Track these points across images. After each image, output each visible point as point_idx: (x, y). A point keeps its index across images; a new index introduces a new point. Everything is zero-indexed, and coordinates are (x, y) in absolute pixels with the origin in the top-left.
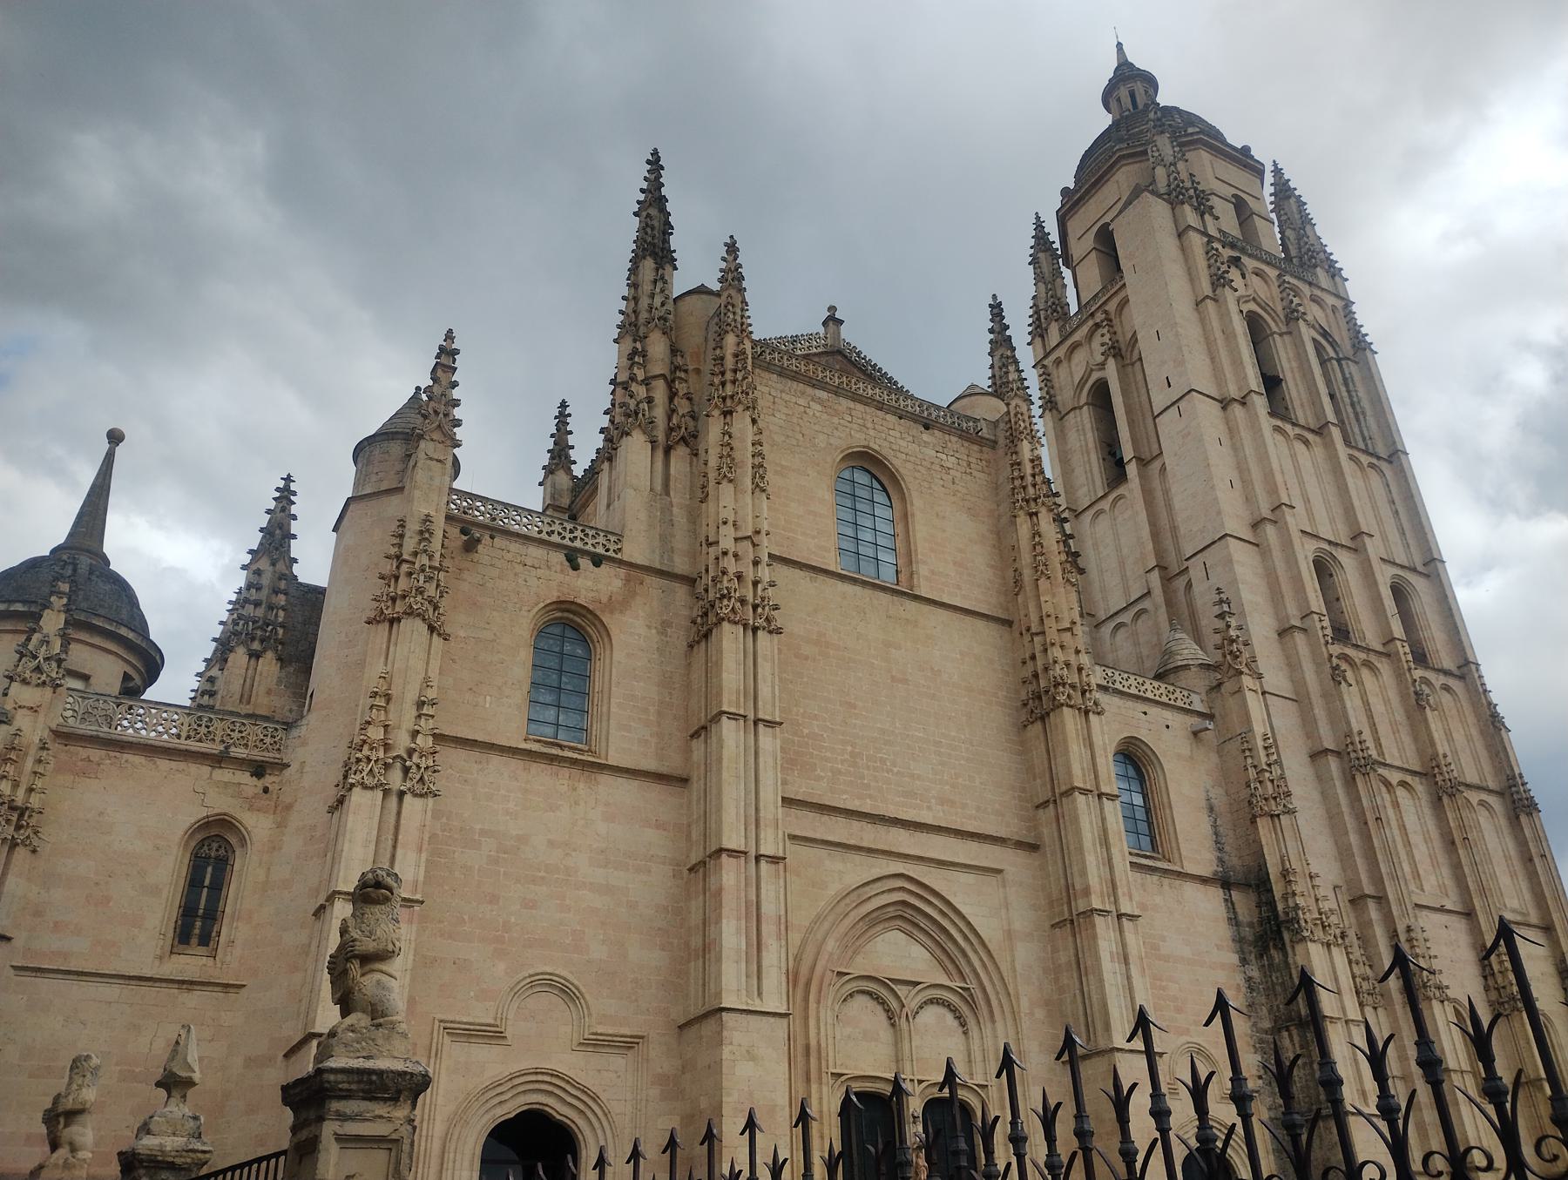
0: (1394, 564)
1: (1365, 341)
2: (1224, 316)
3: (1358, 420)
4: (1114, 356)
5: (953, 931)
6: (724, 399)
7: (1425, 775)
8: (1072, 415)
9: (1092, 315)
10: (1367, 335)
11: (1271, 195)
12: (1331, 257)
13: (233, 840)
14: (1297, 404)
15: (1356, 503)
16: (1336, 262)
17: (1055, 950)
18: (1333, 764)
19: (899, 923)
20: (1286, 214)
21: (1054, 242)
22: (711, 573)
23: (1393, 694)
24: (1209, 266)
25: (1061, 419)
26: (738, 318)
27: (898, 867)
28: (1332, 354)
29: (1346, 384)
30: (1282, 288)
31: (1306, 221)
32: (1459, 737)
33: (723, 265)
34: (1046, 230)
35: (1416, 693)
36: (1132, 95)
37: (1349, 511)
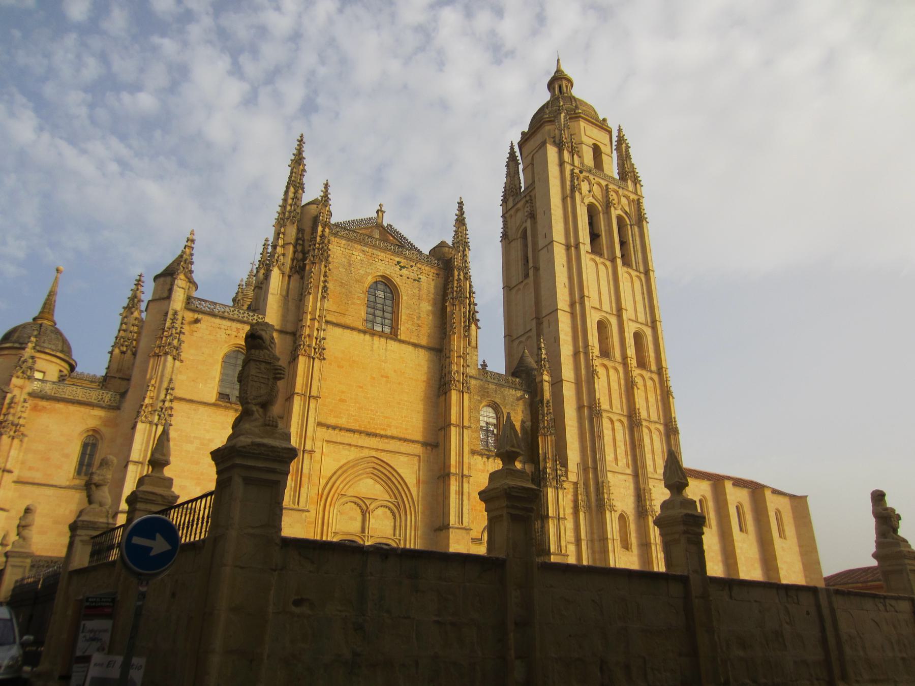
3: (635, 254)
4: (530, 218)
6: (314, 257)
8: (513, 242)
11: (616, 142)
13: (98, 437)
16: (639, 177)
18: (586, 411)
21: (518, 156)
23: (622, 382)
25: (510, 243)
27: (374, 454)
28: (628, 222)
29: (632, 237)
31: (628, 156)
32: (652, 400)
34: (515, 150)
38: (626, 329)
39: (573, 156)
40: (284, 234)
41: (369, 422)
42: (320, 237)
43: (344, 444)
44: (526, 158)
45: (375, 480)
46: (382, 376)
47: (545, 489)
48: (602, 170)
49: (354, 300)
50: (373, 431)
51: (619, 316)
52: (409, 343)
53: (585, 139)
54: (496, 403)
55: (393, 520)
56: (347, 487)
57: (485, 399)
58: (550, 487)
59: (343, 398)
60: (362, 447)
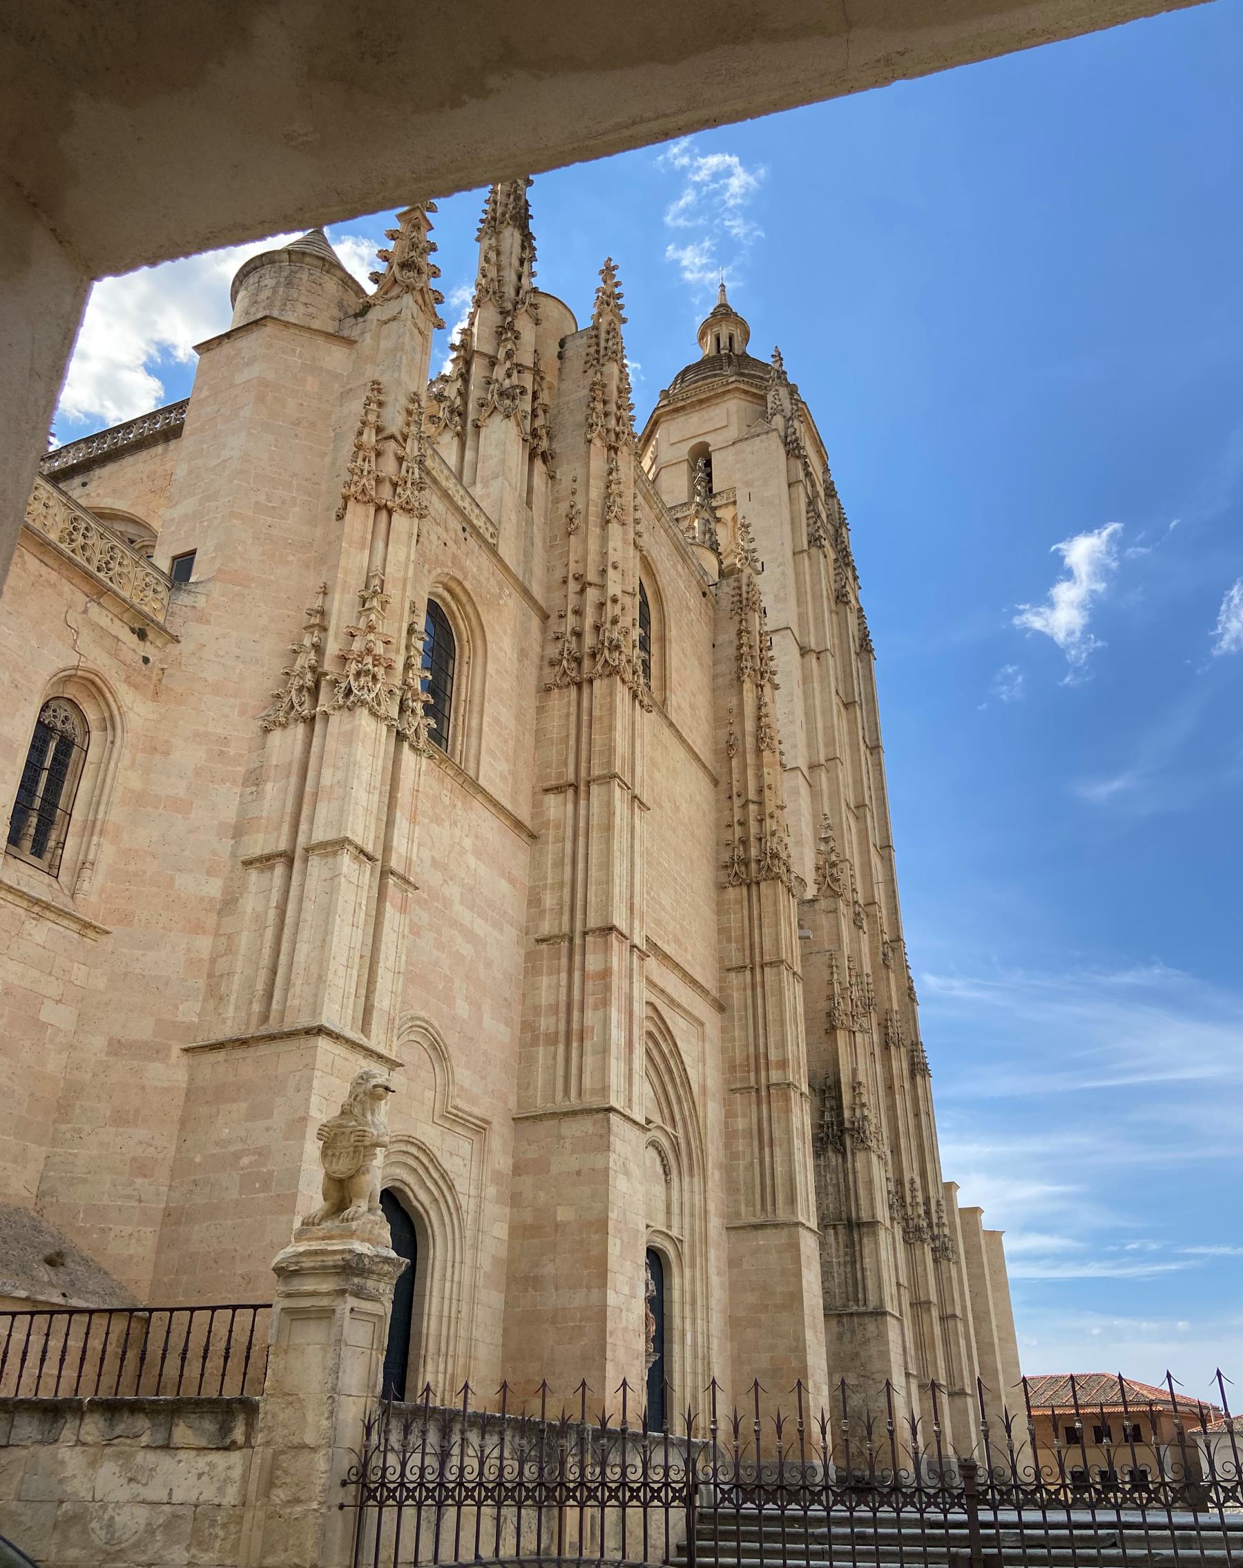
30: (837, 572)
36: (731, 338)
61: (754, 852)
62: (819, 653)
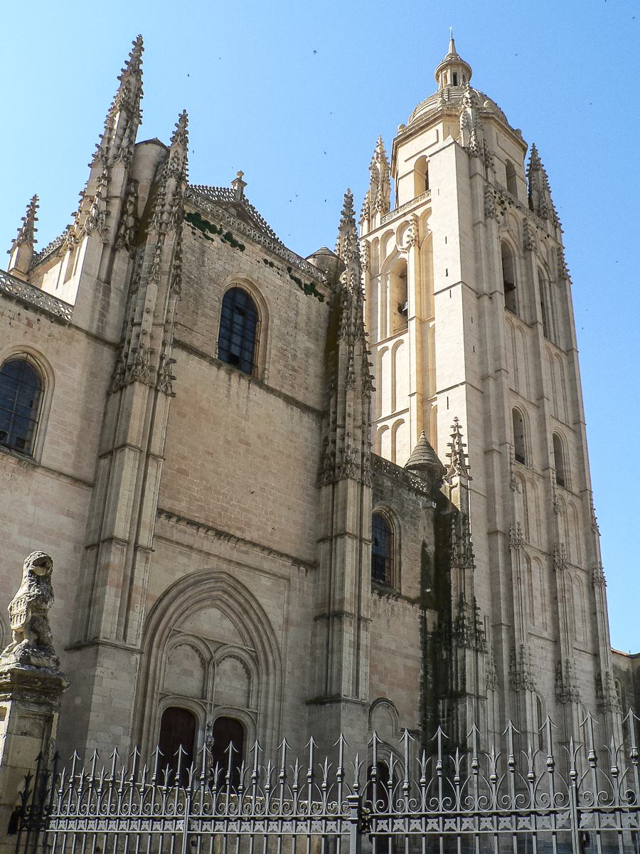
0: (557, 419)
1: (567, 275)
2: (488, 238)
5: (251, 613)
7: (549, 555)
9: (405, 215)
10: (568, 270)
11: (528, 165)
12: (557, 215)
14: (521, 307)
15: (544, 377)
17: (314, 635)
18: (500, 540)
19: (218, 602)
20: (534, 180)
21: (388, 158)
22: (132, 346)
23: (541, 503)
24: (485, 203)
26: (180, 169)
27: (224, 567)
28: (546, 277)
30: (525, 228)
31: (546, 188)
33: (176, 129)
35: (555, 504)
37: (539, 382)
38: (548, 428)
39: (487, 167)
40: (109, 179)
41: (220, 514)
42: (174, 195)
43: (182, 545)
44: (406, 161)
45: (224, 612)
46: (241, 441)
47: (460, 652)
48: (516, 196)
49: (206, 310)
50: (225, 529)
51: (539, 405)
52: (279, 394)
53: (497, 150)
54: (391, 510)
55: (246, 681)
56: (182, 618)
57: (378, 501)
58: (469, 648)
59: (184, 468)
60: (208, 554)
61: (337, 460)
62: (491, 294)
